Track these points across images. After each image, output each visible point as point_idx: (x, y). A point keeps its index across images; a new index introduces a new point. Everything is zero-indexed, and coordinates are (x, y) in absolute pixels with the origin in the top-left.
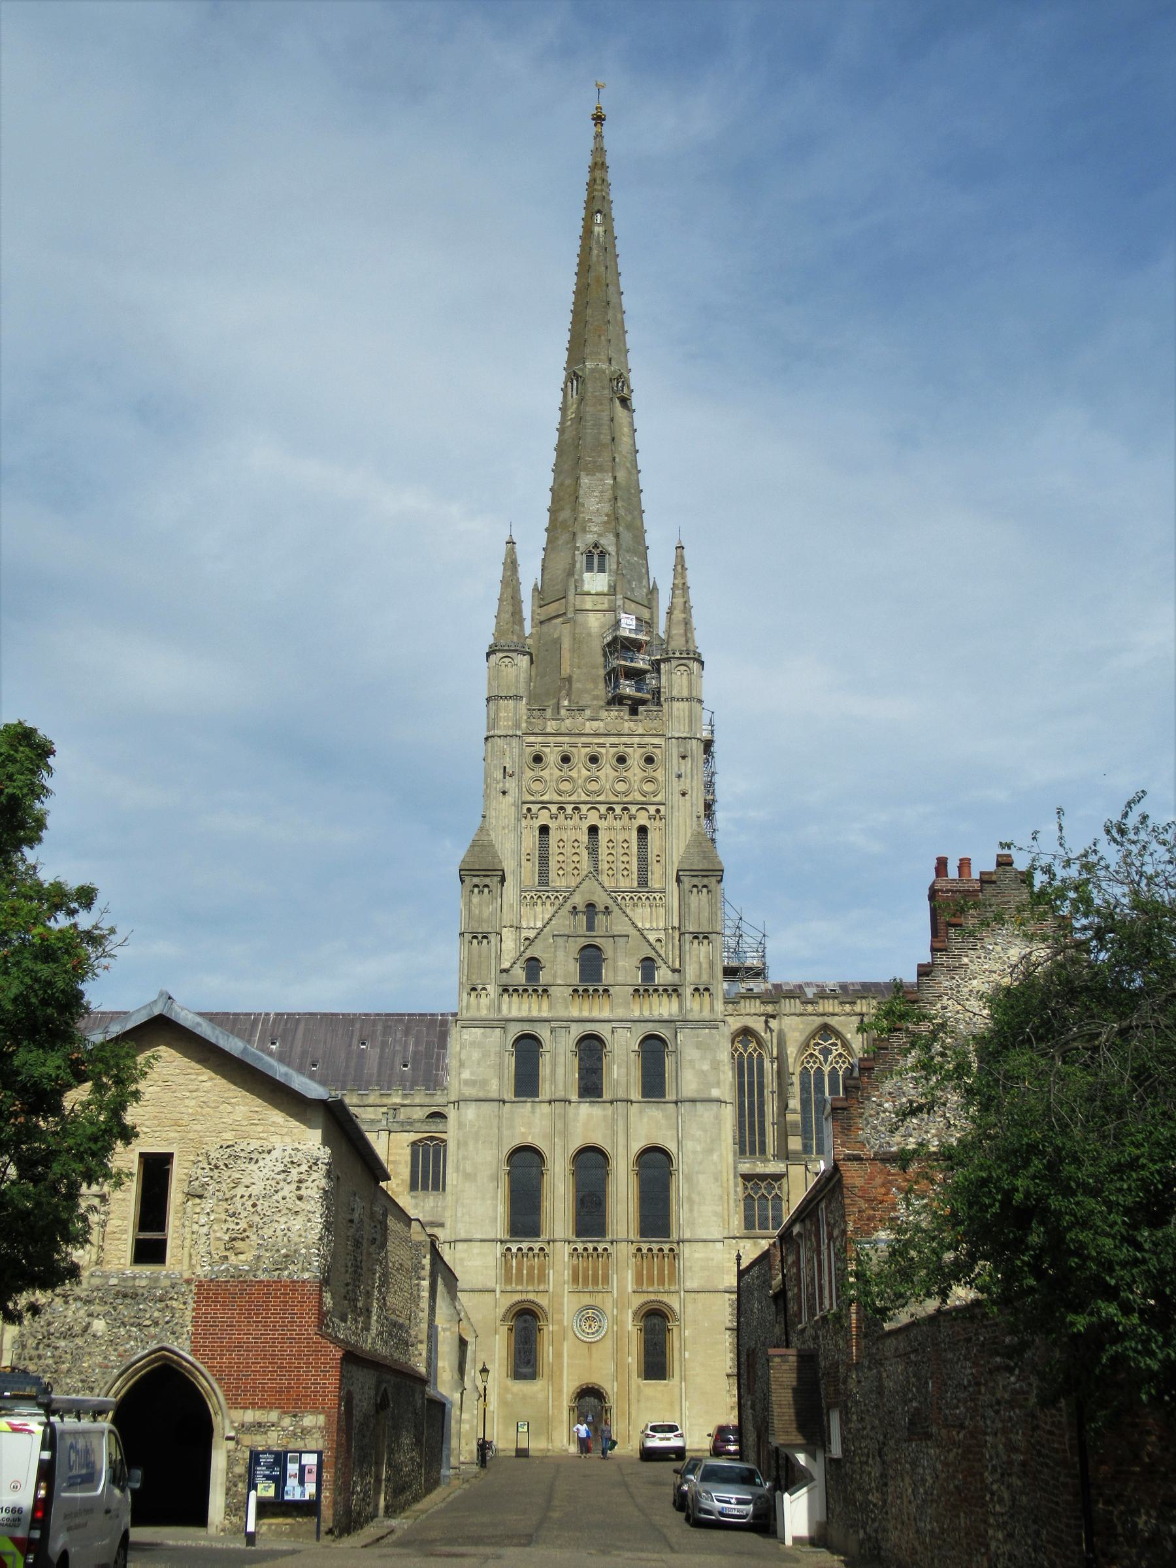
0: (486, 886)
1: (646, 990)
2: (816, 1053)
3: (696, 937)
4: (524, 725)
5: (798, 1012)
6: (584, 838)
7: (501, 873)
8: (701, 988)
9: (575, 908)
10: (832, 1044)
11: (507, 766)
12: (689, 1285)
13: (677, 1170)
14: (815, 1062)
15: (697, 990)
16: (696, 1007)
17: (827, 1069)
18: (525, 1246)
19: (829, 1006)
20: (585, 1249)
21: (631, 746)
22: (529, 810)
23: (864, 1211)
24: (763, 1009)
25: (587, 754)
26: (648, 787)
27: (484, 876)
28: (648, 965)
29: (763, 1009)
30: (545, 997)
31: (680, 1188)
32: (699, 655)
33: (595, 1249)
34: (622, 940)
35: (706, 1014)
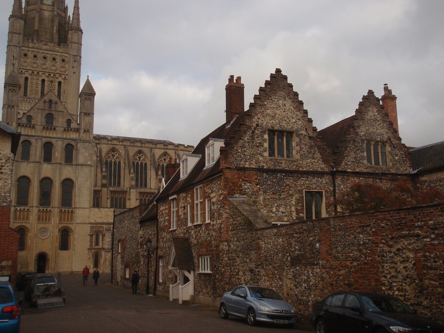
0: (14, 90)
1: (68, 129)
2: (111, 156)
3: (85, 114)
4: (21, 43)
5: (106, 143)
6: (40, 83)
7: (20, 86)
8: (86, 130)
9: (45, 101)
10: (115, 154)
11: (15, 56)
12: (77, 221)
13: (75, 186)
14: (110, 159)
15: (85, 131)
16: (85, 136)
17: (113, 161)
18: (22, 208)
19: (115, 142)
20: (43, 210)
21: (58, 55)
22: (22, 71)
23: (231, 187)
25: (42, 56)
26: (63, 70)
27: (14, 86)
28: (69, 122)
30: (33, 129)
31: (76, 191)
32: (82, 30)
33: (47, 210)
34: (61, 113)
35: (87, 139)
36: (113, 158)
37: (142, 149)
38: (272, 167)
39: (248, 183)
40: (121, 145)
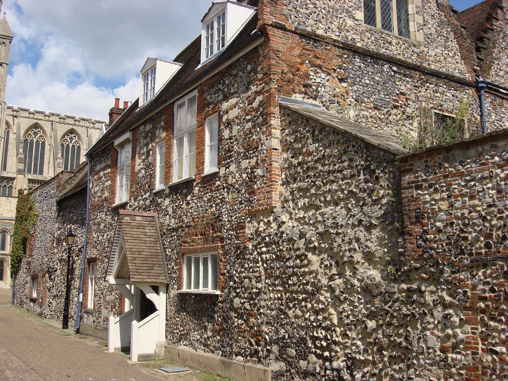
5: (26, 116)
10: (39, 131)
14: (31, 137)
23: (286, 74)
24: (12, 113)
29: (12, 113)
36: (35, 138)
37: (75, 127)
38: (372, 48)
39: (324, 72)
40: (46, 121)
